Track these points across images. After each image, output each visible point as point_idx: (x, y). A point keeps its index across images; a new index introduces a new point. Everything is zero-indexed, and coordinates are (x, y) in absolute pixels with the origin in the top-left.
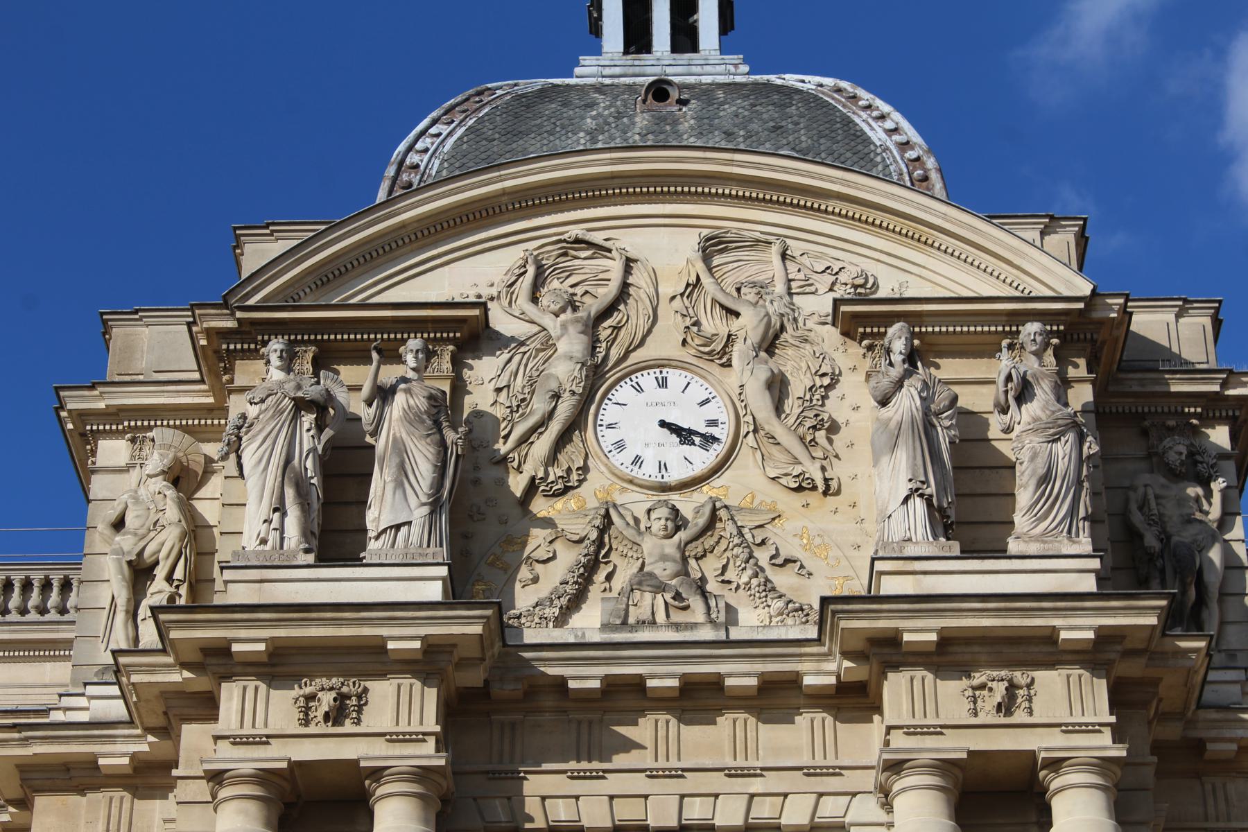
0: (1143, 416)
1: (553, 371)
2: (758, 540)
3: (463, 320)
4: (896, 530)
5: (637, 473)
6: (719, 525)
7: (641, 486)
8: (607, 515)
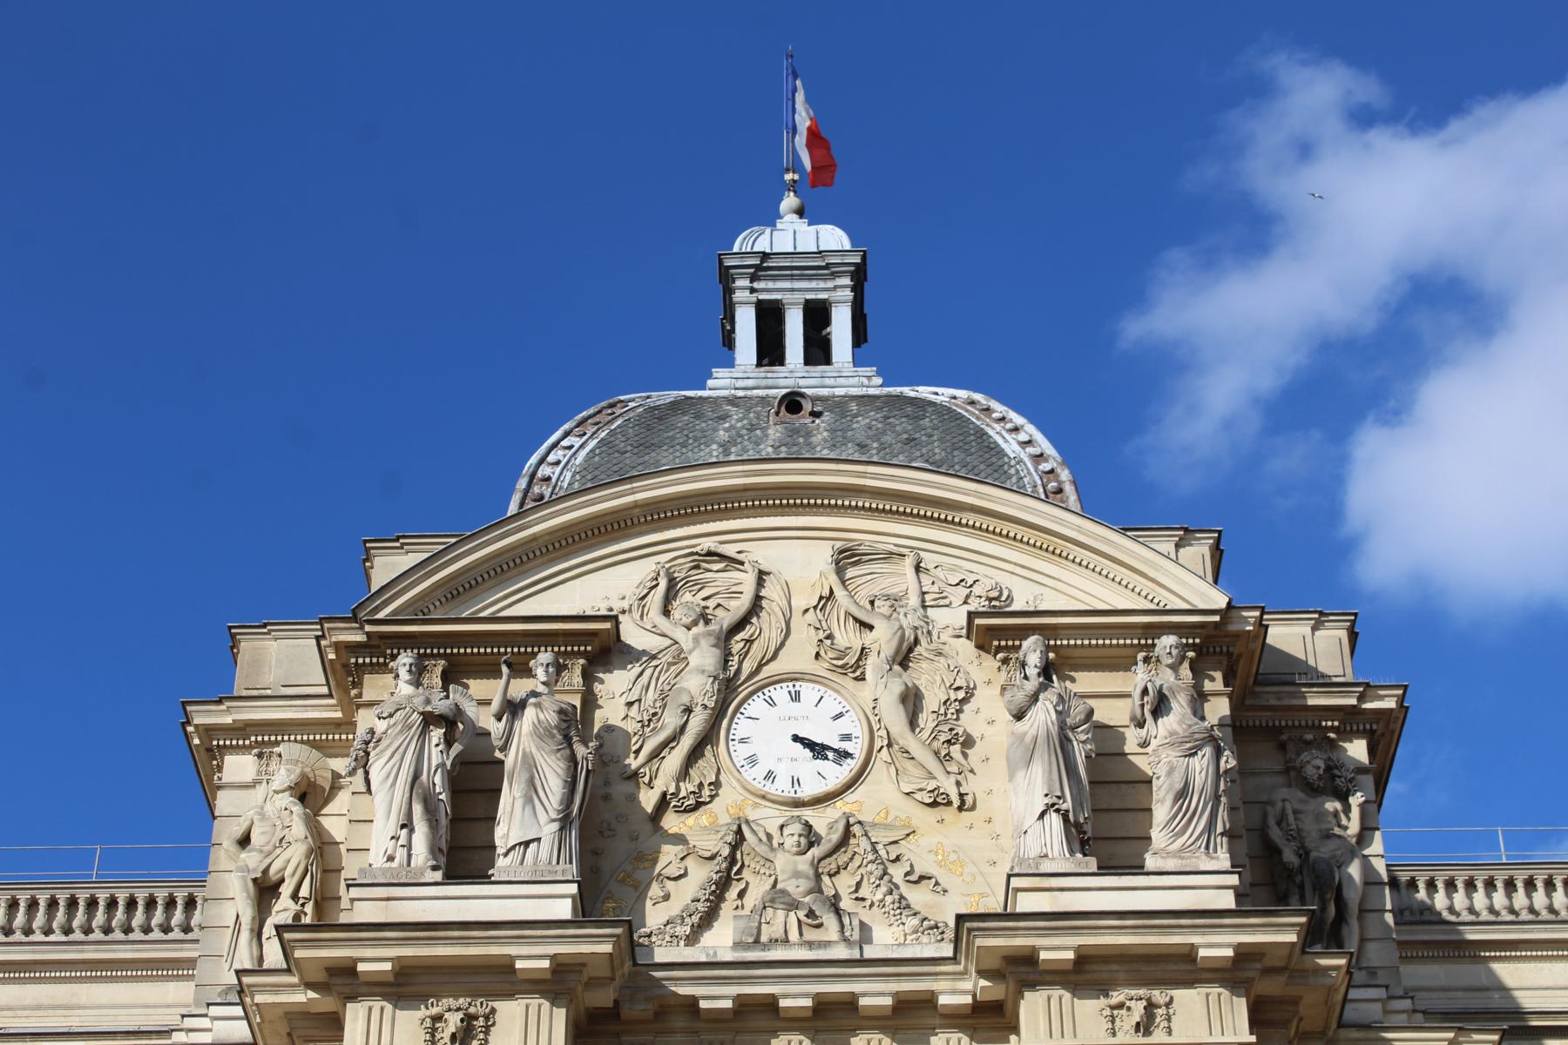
0: (1280, 730)
1: (684, 684)
2: (893, 857)
3: (593, 634)
4: (1032, 847)
5: (769, 788)
6: (852, 841)
7: (773, 802)
8: (739, 831)
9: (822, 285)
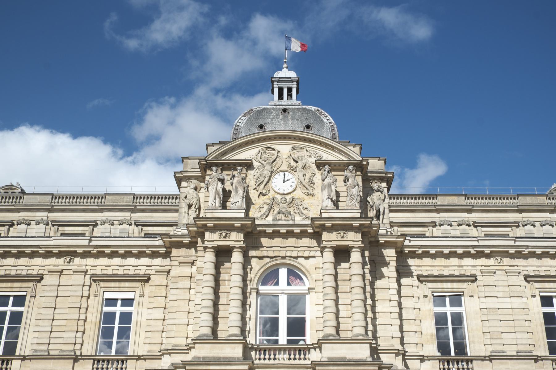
4: (324, 205)
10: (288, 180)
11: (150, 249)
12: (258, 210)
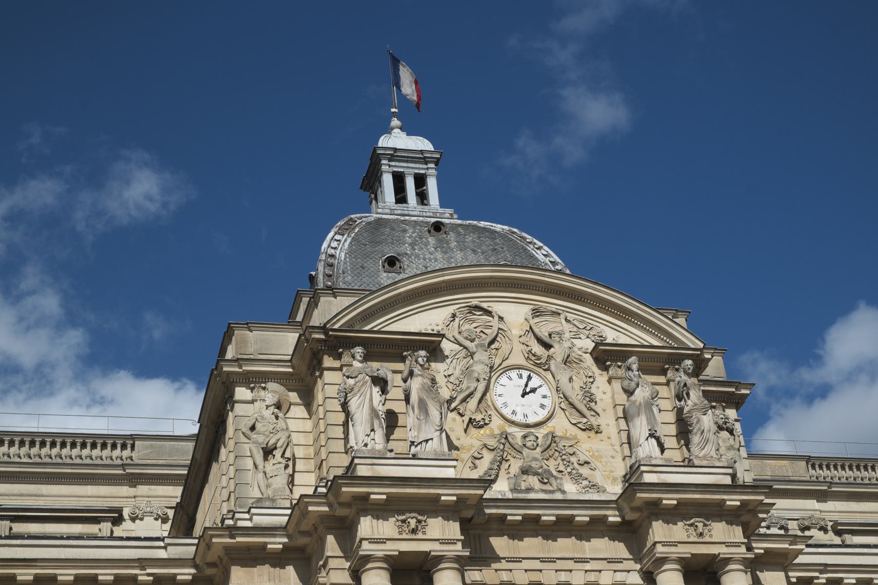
3: (433, 342)
9: (421, 166)
10: (533, 390)
11: (149, 571)
12: (470, 464)
